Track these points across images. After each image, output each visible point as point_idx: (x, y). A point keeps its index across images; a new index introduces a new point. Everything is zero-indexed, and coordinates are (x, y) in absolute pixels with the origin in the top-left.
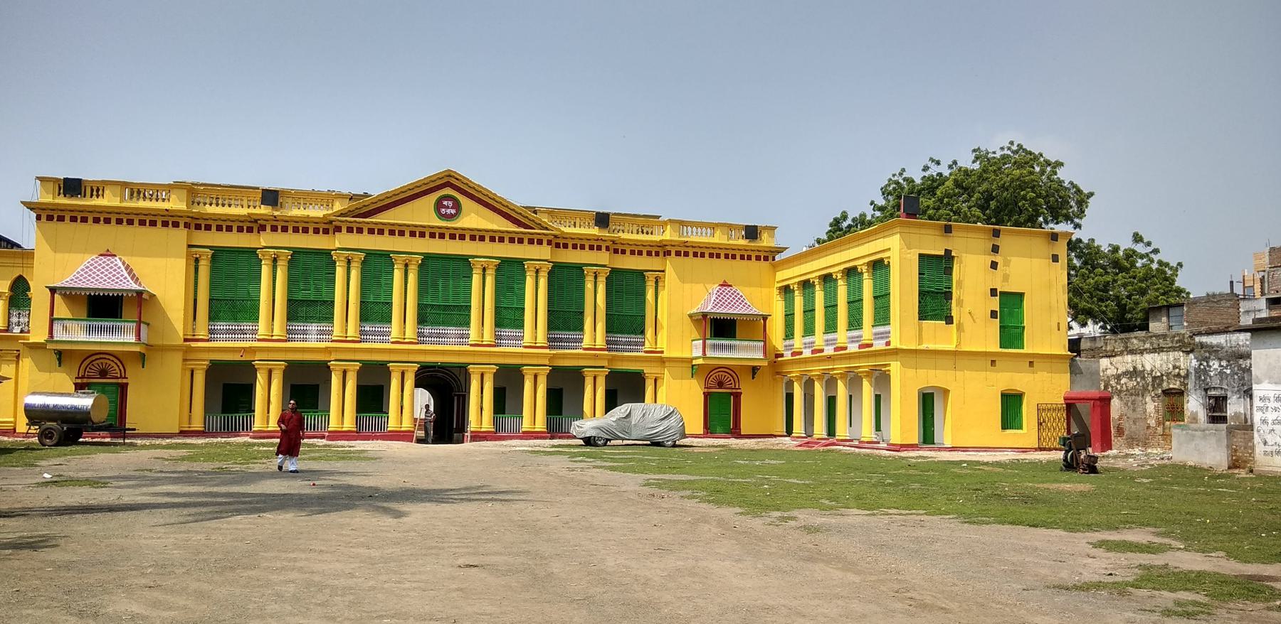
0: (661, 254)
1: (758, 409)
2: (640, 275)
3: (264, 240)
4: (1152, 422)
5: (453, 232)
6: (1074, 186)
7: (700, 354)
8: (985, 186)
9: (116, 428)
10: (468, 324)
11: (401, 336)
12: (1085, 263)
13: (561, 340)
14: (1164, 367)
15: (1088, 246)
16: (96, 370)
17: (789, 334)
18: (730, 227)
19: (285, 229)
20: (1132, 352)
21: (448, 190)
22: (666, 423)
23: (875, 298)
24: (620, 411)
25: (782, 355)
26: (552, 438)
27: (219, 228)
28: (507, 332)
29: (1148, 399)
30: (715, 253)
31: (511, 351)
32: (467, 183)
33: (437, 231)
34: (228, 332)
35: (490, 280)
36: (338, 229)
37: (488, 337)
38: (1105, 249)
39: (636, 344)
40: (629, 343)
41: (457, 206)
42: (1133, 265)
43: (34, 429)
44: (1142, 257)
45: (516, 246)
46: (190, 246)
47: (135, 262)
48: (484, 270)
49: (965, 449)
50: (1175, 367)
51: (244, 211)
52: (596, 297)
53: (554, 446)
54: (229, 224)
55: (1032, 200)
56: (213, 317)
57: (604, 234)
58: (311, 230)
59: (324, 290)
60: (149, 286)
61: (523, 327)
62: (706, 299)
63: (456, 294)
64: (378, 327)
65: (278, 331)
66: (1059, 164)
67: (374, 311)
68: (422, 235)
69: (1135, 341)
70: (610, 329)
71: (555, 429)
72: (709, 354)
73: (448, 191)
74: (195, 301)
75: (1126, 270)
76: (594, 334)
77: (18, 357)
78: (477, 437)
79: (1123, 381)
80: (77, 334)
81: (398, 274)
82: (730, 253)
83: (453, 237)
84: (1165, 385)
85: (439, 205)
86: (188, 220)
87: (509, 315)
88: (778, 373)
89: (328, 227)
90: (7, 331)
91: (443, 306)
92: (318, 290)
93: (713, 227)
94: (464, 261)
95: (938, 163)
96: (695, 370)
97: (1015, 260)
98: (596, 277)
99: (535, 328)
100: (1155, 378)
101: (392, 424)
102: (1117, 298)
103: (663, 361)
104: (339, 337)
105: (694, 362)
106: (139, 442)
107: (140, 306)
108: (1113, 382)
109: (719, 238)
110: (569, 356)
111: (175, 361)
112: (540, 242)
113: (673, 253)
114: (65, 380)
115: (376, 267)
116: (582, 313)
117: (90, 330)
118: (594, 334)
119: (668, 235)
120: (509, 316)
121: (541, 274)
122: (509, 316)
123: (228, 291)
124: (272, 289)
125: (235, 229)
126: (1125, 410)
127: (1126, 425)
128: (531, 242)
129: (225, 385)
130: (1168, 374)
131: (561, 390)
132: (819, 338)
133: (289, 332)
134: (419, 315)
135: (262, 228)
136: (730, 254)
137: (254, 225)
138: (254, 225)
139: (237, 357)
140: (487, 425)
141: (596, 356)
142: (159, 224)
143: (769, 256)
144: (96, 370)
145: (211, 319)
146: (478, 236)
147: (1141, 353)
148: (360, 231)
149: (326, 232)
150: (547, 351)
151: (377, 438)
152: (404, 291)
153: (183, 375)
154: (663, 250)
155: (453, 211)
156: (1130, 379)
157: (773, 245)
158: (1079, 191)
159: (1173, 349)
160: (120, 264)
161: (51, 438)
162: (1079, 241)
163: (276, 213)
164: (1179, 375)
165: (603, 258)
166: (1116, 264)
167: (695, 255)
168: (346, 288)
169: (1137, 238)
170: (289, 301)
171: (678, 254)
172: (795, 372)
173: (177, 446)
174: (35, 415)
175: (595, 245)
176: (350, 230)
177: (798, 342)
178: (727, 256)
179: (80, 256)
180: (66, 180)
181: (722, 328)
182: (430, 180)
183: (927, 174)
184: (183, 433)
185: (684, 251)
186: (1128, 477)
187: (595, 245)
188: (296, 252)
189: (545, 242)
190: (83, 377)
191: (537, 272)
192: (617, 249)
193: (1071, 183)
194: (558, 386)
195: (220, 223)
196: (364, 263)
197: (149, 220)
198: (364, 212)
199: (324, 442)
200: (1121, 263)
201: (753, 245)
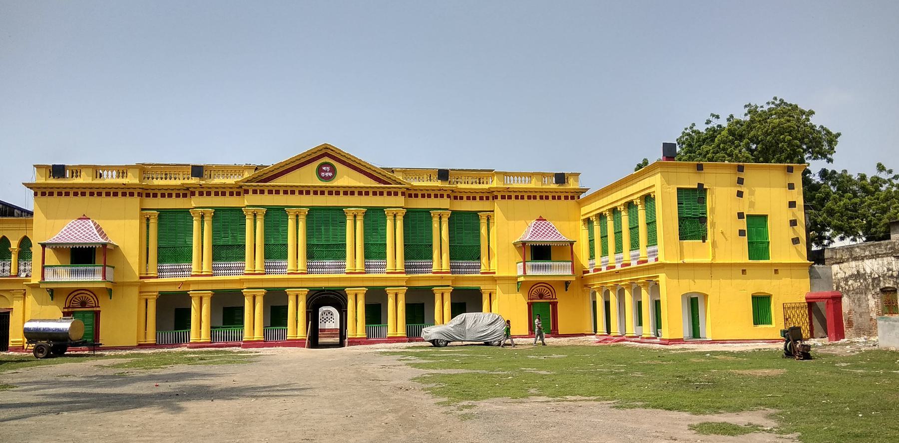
0: (491, 198)
1: (568, 316)
2: (475, 215)
3: (193, 202)
4: (873, 315)
5: (330, 189)
6: (824, 129)
7: (522, 273)
8: (752, 133)
9: (92, 343)
10: (344, 257)
11: (296, 270)
12: (838, 189)
13: (416, 267)
14: (881, 270)
15: (841, 176)
16: (78, 303)
17: (592, 257)
18: (543, 175)
19: (209, 194)
20: (856, 259)
21: (326, 158)
22: (492, 328)
23: (648, 224)
24: (459, 318)
25: (588, 272)
26: (410, 341)
27: (163, 196)
28: (373, 262)
29: (870, 296)
30: (531, 195)
31: (376, 277)
32: (339, 152)
33: (319, 190)
34: (171, 270)
35: (359, 224)
36: (246, 192)
37: (359, 266)
38: (855, 177)
39: (474, 267)
40: (469, 267)
41: (333, 170)
42: (877, 189)
43: (31, 347)
44: (885, 182)
45: (378, 197)
46: (143, 209)
47: (102, 223)
48: (355, 216)
49: (723, 342)
50: (889, 270)
51: (178, 182)
52: (440, 233)
53: (409, 348)
54: (170, 192)
55: (789, 142)
56: (160, 260)
57: (446, 185)
58: (227, 194)
59: (239, 237)
60: (113, 240)
61: (385, 258)
62: (526, 231)
65: (206, 268)
66: (812, 113)
67: (275, 251)
68: (308, 193)
69: (858, 250)
70: (452, 257)
71: (412, 335)
72: (529, 273)
74: (148, 249)
75: (872, 194)
76: (440, 261)
77: (25, 294)
78: (354, 342)
79: (850, 282)
80: (64, 276)
81: (291, 223)
82: (544, 195)
83: (330, 193)
84: (882, 285)
85: (319, 170)
86: (140, 191)
87: (373, 249)
88: (586, 286)
89: (239, 191)
90: (16, 276)
92: (234, 237)
93: (530, 175)
94: (340, 210)
95: (718, 117)
96: (521, 286)
97: (759, 191)
98: (440, 218)
99: (394, 257)
100: (874, 279)
101: (290, 335)
102: (864, 216)
103: (495, 280)
104: (250, 271)
106: (107, 353)
107: (105, 255)
108: (842, 284)
109: (534, 184)
110: (421, 279)
111: (135, 291)
112: (396, 194)
113: (499, 197)
114: (56, 310)
115: (275, 218)
116: (431, 245)
117: (72, 273)
118: (440, 261)
119: (495, 183)
120: (374, 250)
121: (398, 218)
122: (374, 250)
123: (170, 238)
124: (201, 238)
125: (174, 195)
126: (853, 305)
127: (854, 318)
128: (389, 194)
129: (177, 310)
130: (884, 276)
131: (423, 305)
132: (611, 258)
133: (214, 269)
134: (308, 252)
135: (193, 194)
136: (544, 196)
137: (186, 192)
138: (186, 192)
141: (442, 277)
142: (120, 194)
143: (574, 195)
144: (78, 303)
145: (159, 262)
146: (349, 192)
147: (863, 259)
148: (262, 192)
149: (238, 194)
150: (404, 275)
152: (296, 236)
153: (139, 303)
154: (491, 195)
155: (330, 174)
156: (855, 280)
157: (577, 187)
158: (828, 133)
159: (887, 255)
160: (92, 225)
161: (42, 352)
162: (834, 172)
163: (202, 182)
164: (892, 276)
165: (445, 203)
166: (864, 189)
167: (517, 198)
168: (254, 235)
169: (881, 168)
170: (213, 246)
171: (503, 197)
172: (596, 283)
173: (134, 355)
174: (32, 335)
175: (439, 194)
176: (255, 192)
177: (598, 261)
178: (541, 198)
179: (63, 221)
180: (54, 166)
181: (540, 252)
182: (308, 154)
183: (709, 126)
184: (141, 346)
185: (507, 195)
186: (832, 360)
187: (439, 194)
189: (400, 194)
190: (69, 307)
191: (395, 216)
192: (456, 196)
193: (822, 127)
195: (163, 192)
196: (266, 215)
197: (112, 192)
198: (264, 178)
199: (240, 349)
200: (870, 187)
201: (562, 188)
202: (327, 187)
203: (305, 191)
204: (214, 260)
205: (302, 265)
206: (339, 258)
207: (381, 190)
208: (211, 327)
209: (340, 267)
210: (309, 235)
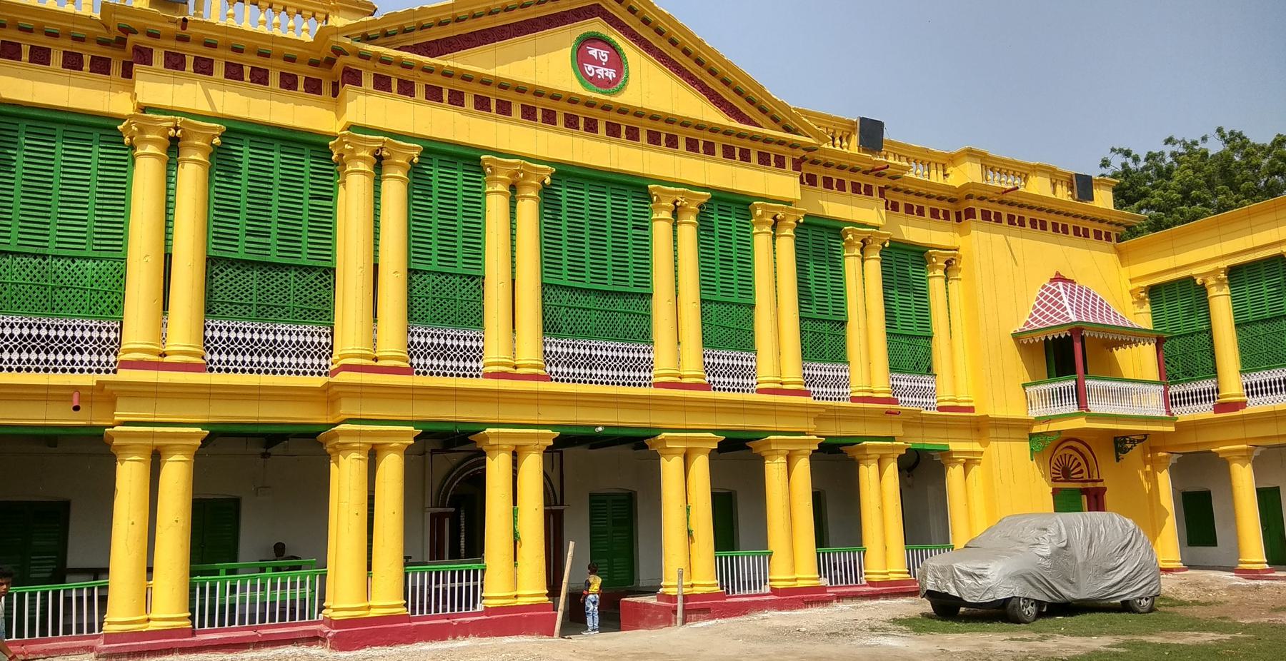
28: (726, 357)
36: (353, 77)
41: (617, 61)
63: (621, 266)
64: (455, 337)
72: (1095, 407)
73: (596, 26)
89: (326, 72)
91: (595, 299)
94: (636, 188)
103: (982, 427)
105: (1036, 429)
112: (780, 163)
139: (59, 416)
140: (705, 579)
146: (663, 132)
152: (511, 247)
155: (611, 74)
168: (367, 229)
176: (382, 84)
188: (238, 131)
189: (789, 164)
194: (726, 487)
202: (607, 108)
203: (540, 107)
204: (210, 309)
205: (529, 350)
206: (634, 340)
207: (746, 144)
208: (192, 574)
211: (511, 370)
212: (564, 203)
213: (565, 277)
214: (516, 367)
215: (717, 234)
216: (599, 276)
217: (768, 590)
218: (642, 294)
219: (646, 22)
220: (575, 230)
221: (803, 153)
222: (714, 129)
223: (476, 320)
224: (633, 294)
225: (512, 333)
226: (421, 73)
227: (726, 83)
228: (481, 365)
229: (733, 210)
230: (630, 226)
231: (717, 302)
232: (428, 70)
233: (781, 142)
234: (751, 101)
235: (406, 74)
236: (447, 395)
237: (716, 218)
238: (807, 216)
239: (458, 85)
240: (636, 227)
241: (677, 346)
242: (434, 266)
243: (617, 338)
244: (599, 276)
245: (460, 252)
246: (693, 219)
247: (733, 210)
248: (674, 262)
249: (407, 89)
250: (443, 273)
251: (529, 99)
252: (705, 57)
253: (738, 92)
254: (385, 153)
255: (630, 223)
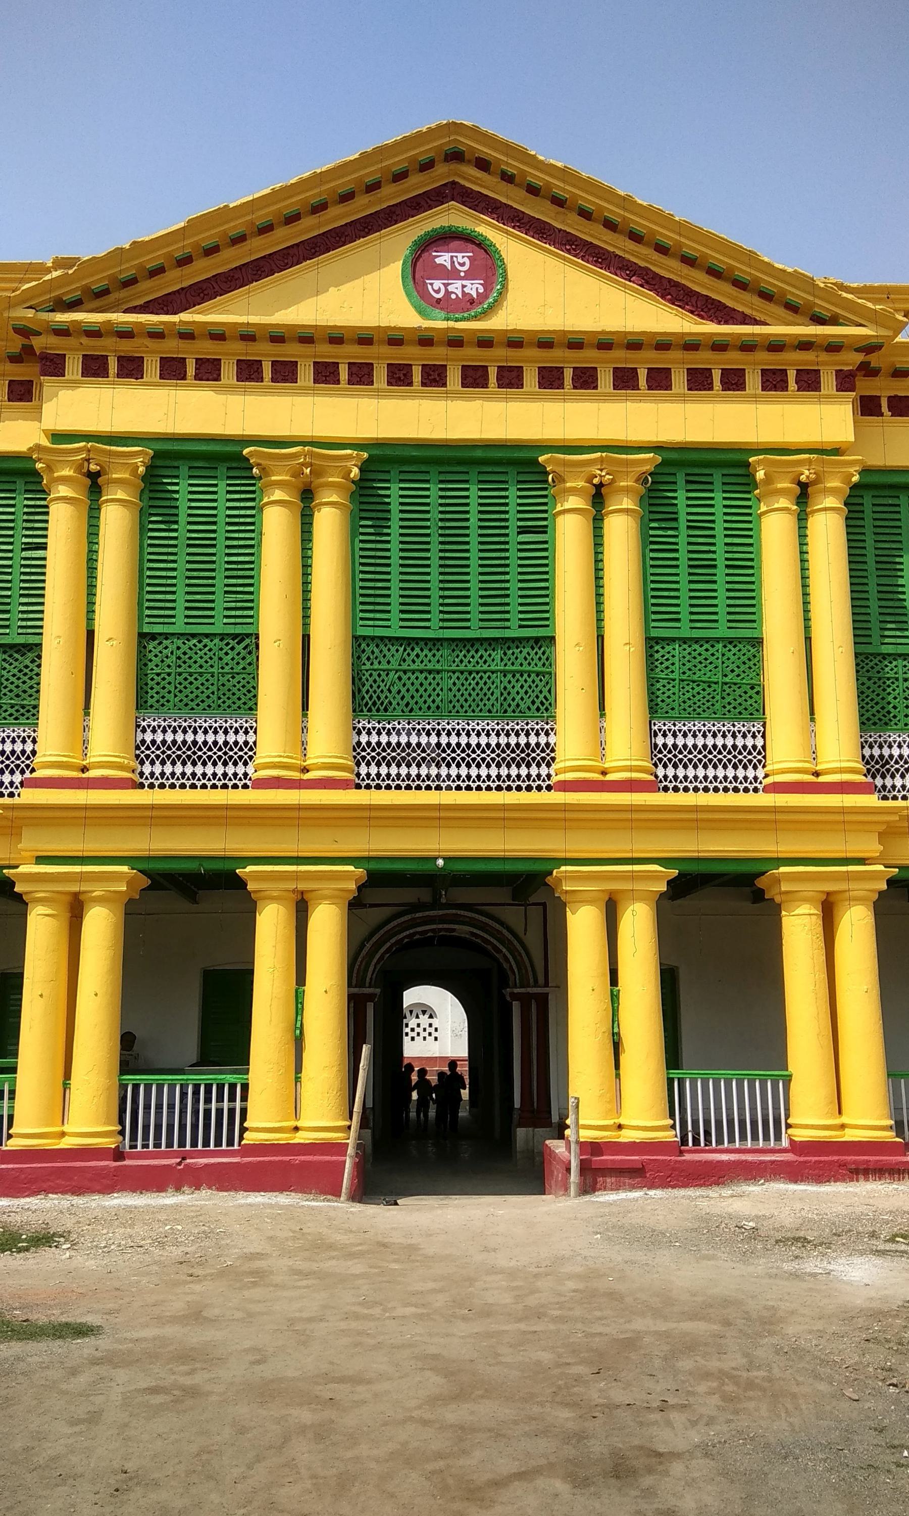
10: (544, 706)
28: (695, 734)
36: (54, 366)
41: (489, 266)
63: (495, 596)
73: (453, 216)
78: (606, 1166)
85: (418, 268)
94: (520, 464)
101: (264, 1120)
112: (809, 382)
128: (774, 381)
134: (357, 680)
150: (871, 800)
151: (195, 1179)
152: (301, 585)
155: (474, 288)
176: (95, 368)
189: (828, 381)
202: (456, 342)
206: (518, 713)
209: (526, 756)
210: (366, 589)
211: (296, 775)
212: (395, 508)
213: (395, 622)
214: (305, 770)
215: (683, 524)
216: (455, 613)
217: (785, 1143)
218: (537, 640)
219: (533, 190)
220: (415, 550)
221: (859, 358)
222: (663, 344)
223: (246, 701)
224: (520, 640)
225: (299, 721)
226: (148, 342)
227: (689, 261)
228: (250, 770)
229: (717, 479)
230: (512, 531)
231: (684, 640)
232: (157, 335)
233: (805, 345)
234: (740, 285)
235: (127, 347)
236: (713, 819)
237: (681, 496)
238: (865, 471)
239: (208, 350)
240: (523, 531)
241: (598, 723)
242: (179, 626)
243: (490, 714)
244: (455, 613)
245: (220, 601)
246: (627, 503)
247: (717, 479)
248: (594, 584)
249: (131, 369)
250: (193, 636)
251: (326, 352)
252: (641, 224)
253: (714, 273)
254: (93, 467)
255: (513, 525)
